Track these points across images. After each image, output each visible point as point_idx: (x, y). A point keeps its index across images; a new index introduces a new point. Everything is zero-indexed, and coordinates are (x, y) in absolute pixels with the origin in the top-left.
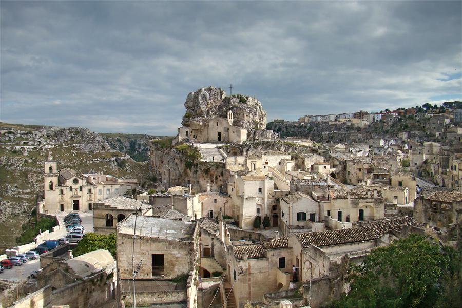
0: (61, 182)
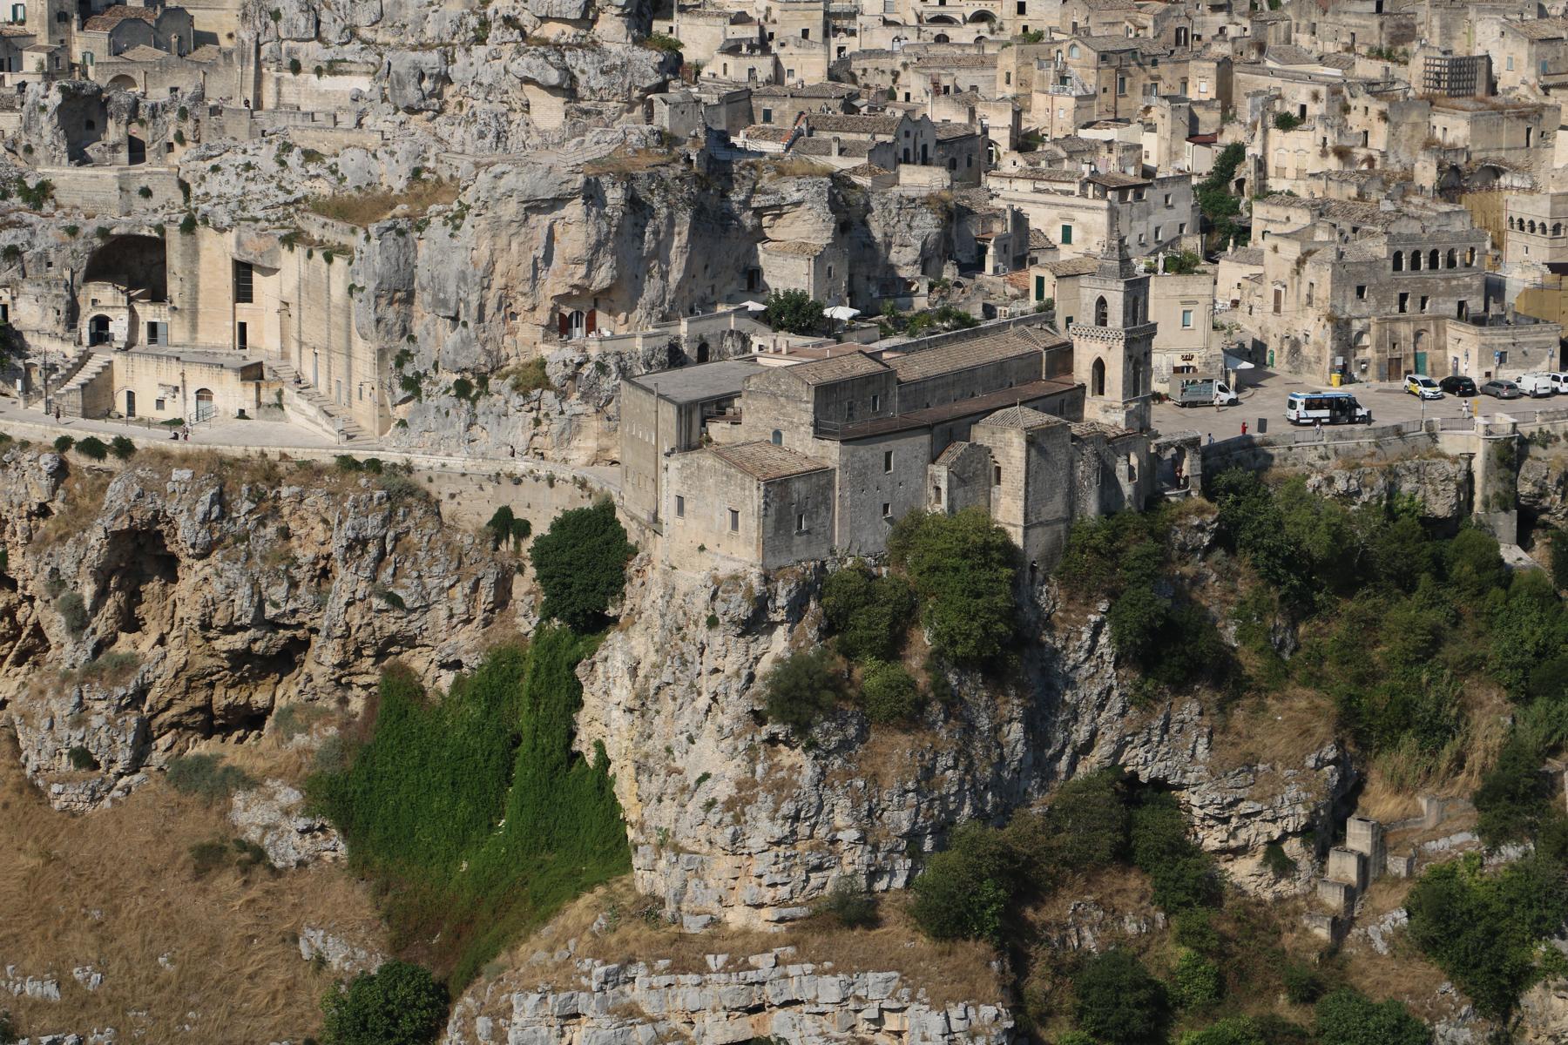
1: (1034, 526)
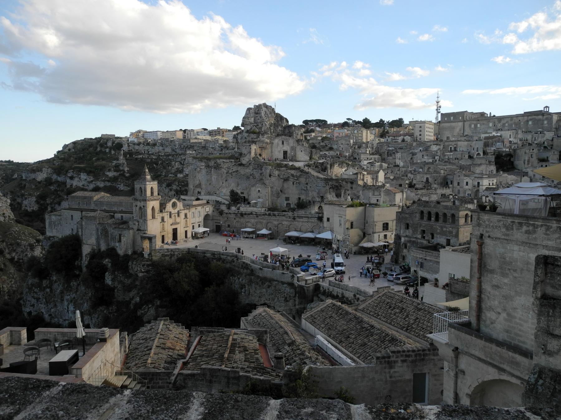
0: (162, 207)
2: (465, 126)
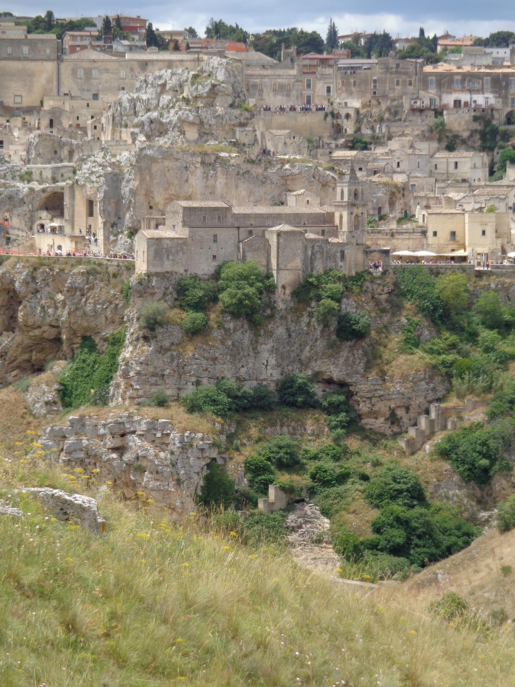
1: (281, 269)
2: (62, 71)
